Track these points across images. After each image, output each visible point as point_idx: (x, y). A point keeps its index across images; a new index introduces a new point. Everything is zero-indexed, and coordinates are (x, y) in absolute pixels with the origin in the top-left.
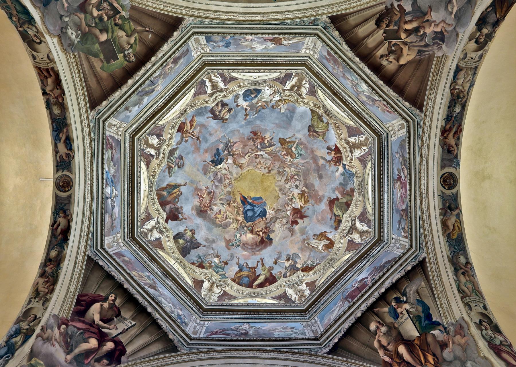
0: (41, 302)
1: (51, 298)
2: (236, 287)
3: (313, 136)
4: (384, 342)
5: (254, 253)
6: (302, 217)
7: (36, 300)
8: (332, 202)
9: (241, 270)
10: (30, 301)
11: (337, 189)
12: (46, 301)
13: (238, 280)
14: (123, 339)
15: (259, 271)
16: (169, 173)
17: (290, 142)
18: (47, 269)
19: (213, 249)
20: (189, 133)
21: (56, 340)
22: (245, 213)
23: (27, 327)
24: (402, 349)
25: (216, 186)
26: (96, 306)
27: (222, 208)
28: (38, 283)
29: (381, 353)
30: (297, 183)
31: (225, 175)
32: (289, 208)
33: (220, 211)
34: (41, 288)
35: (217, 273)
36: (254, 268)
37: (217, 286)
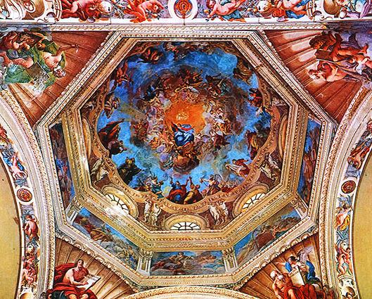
2: (171, 204)
3: (238, 77)
4: (279, 285)
5: (183, 173)
6: (224, 144)
8: (250, 135)
9: (174, 189)
11: (256, 124)
13: (172, 198)
14: (94, 290)
15: (188, 189)
16: (107, 115)
17: (215, 80)
19: (150, 172)
20: (122, 77)
22: (176, 139)
24: (291, 292)
25: (150, 118)
26: (70, 272)
27: (157, 136)
29: (276, 293)
30: (221, 114)
31: (157, 107)
32: (213, 135)
33: (154, 138)
35: (155, 193)
36: (184, 186)
37: (156, 205)
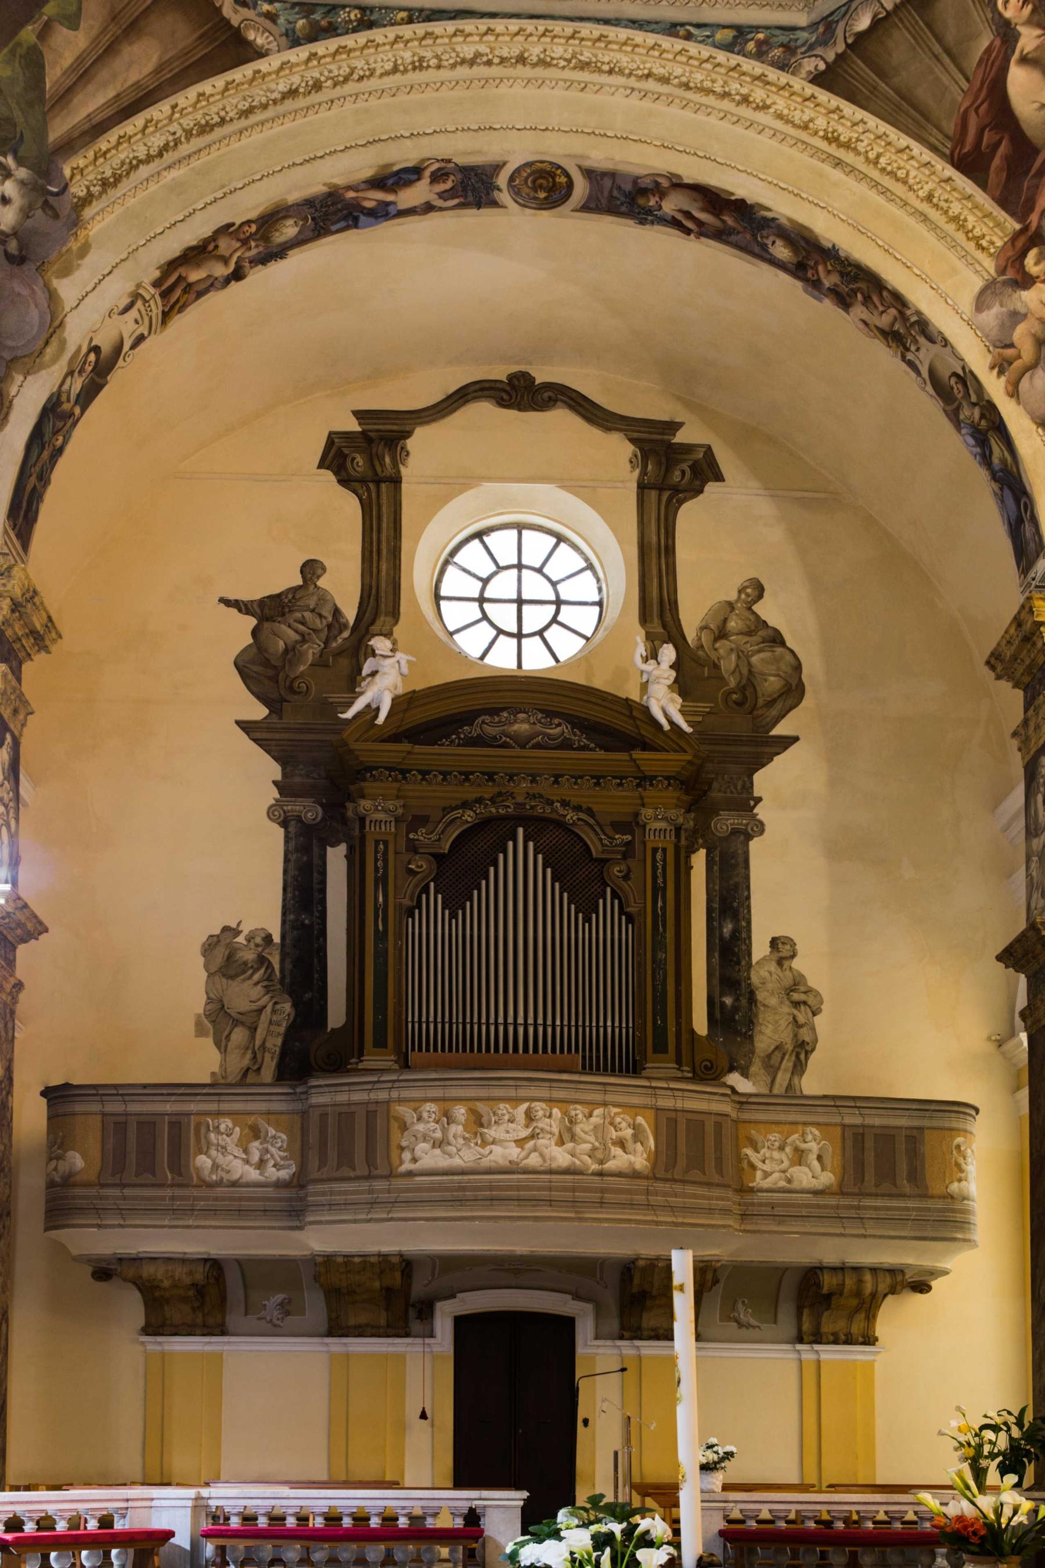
0: (922, 340)
1: (918, 313)
7: (913, 348)
10: (911, 364)
12: (923, 326)
18: (827, 282)
23: (977, 412)
34: (884, 321)
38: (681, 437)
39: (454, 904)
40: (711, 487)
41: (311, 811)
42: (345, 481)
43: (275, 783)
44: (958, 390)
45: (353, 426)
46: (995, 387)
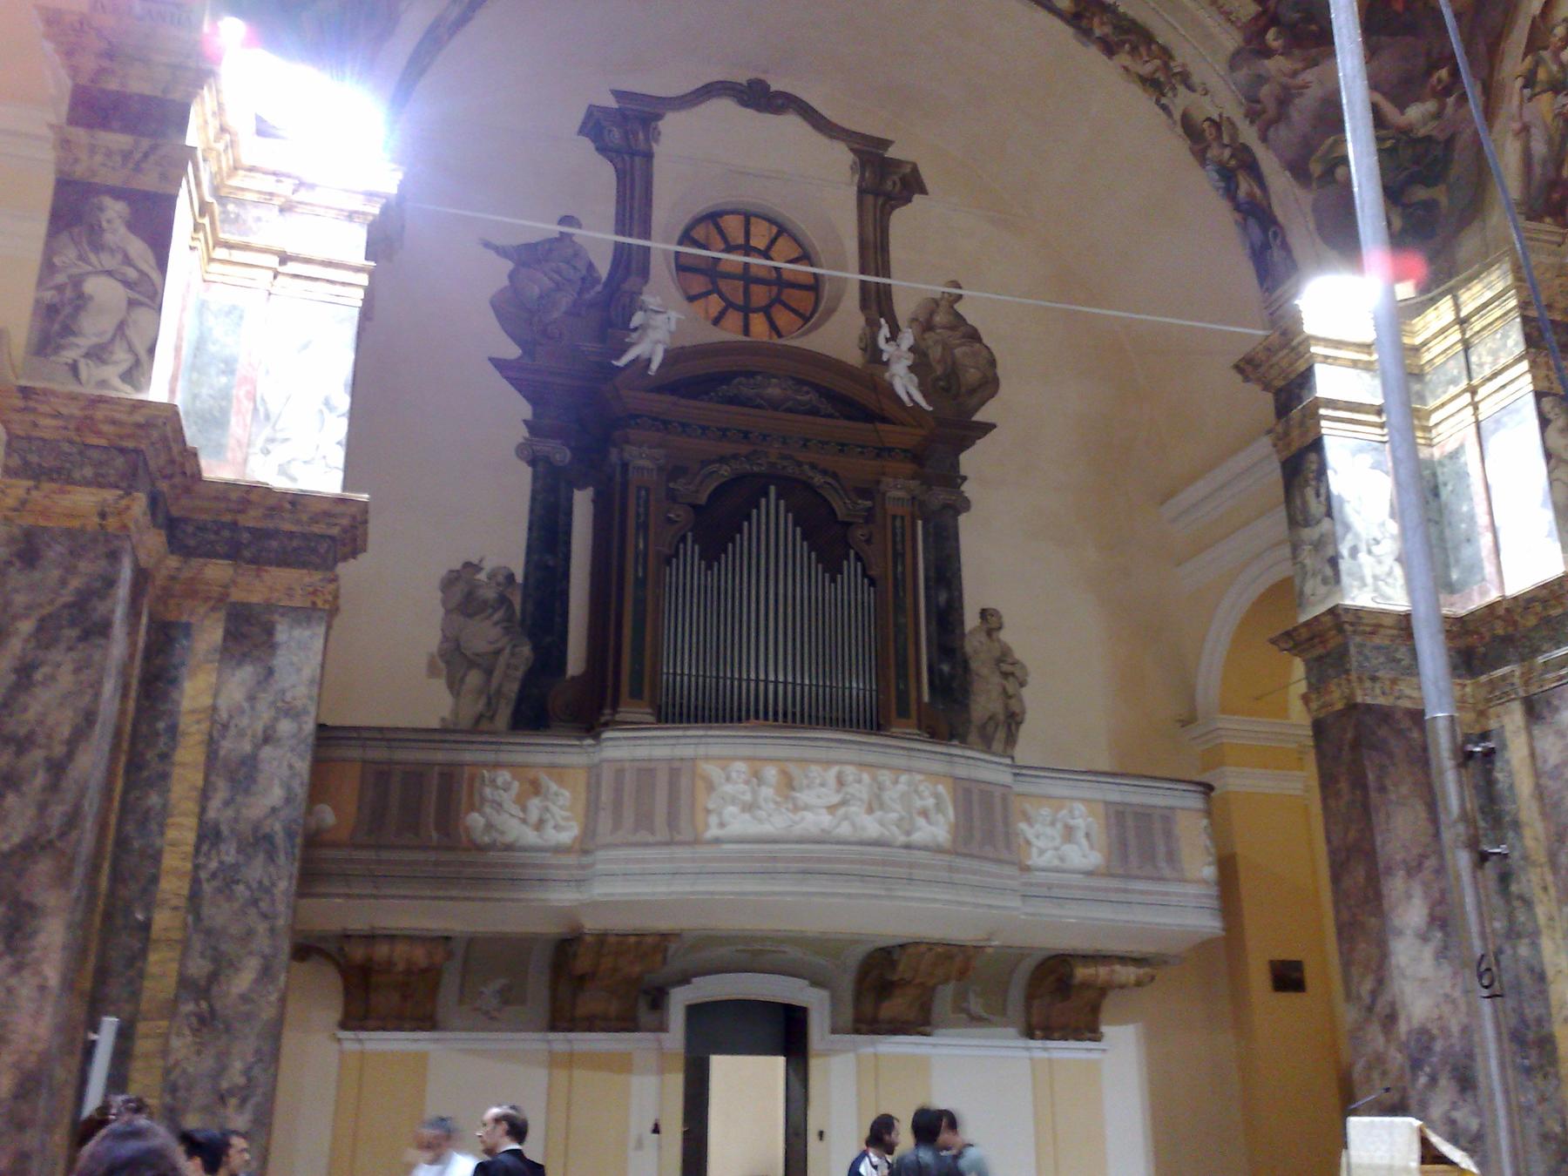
0: (1181, 89)
7: (1170, 94)
10: (1164, 108)
18: (1098, 32)
21: (1295, 74)
23: (1227, 153)
28: (1126, 69)
38: (891, 153)
39: (712, 554)
40: (917, 198)
41: (562, 455)
42: (603, 149)
43: (526, 422)
44: (1210, 133)
45: (612, 103)
46: (1249, 134)
